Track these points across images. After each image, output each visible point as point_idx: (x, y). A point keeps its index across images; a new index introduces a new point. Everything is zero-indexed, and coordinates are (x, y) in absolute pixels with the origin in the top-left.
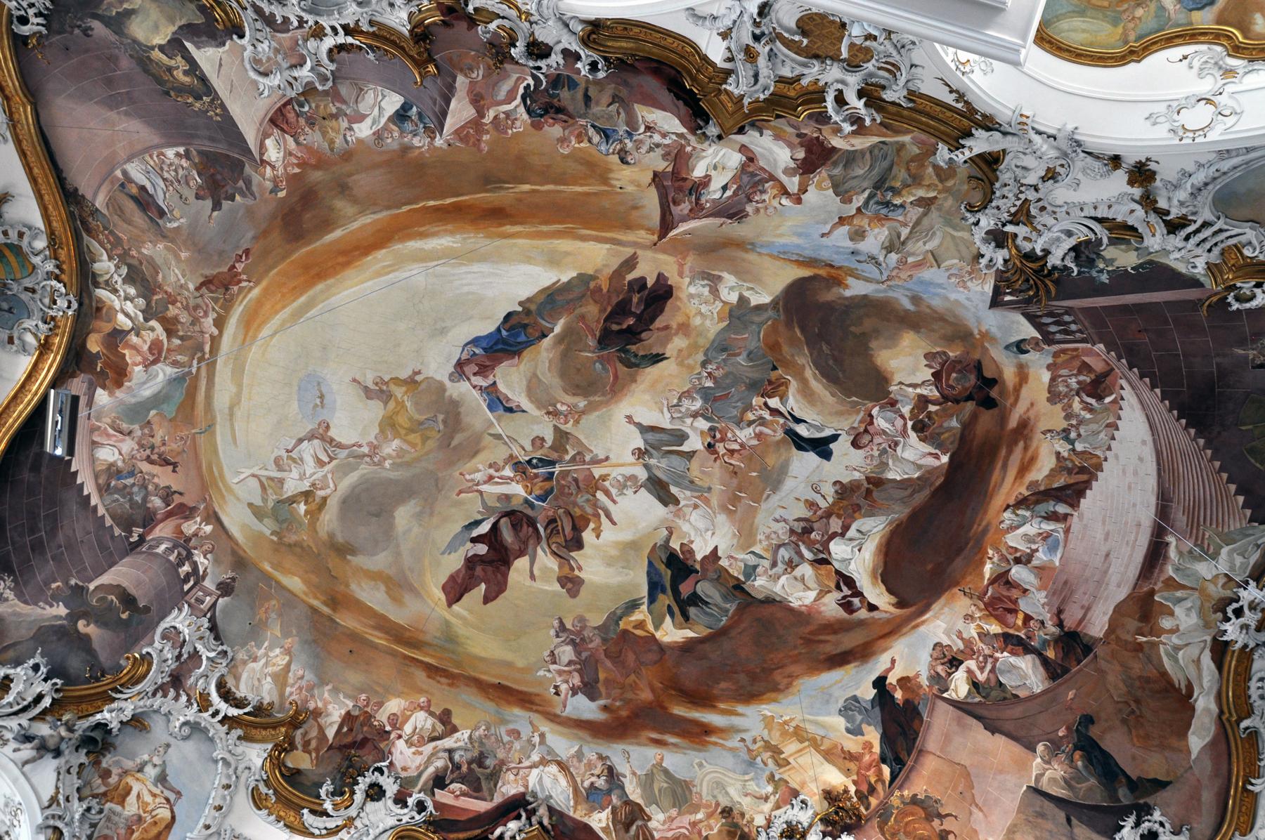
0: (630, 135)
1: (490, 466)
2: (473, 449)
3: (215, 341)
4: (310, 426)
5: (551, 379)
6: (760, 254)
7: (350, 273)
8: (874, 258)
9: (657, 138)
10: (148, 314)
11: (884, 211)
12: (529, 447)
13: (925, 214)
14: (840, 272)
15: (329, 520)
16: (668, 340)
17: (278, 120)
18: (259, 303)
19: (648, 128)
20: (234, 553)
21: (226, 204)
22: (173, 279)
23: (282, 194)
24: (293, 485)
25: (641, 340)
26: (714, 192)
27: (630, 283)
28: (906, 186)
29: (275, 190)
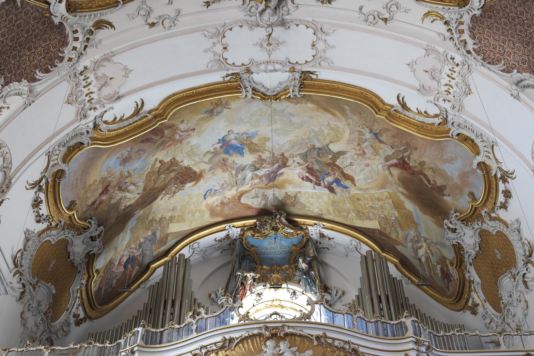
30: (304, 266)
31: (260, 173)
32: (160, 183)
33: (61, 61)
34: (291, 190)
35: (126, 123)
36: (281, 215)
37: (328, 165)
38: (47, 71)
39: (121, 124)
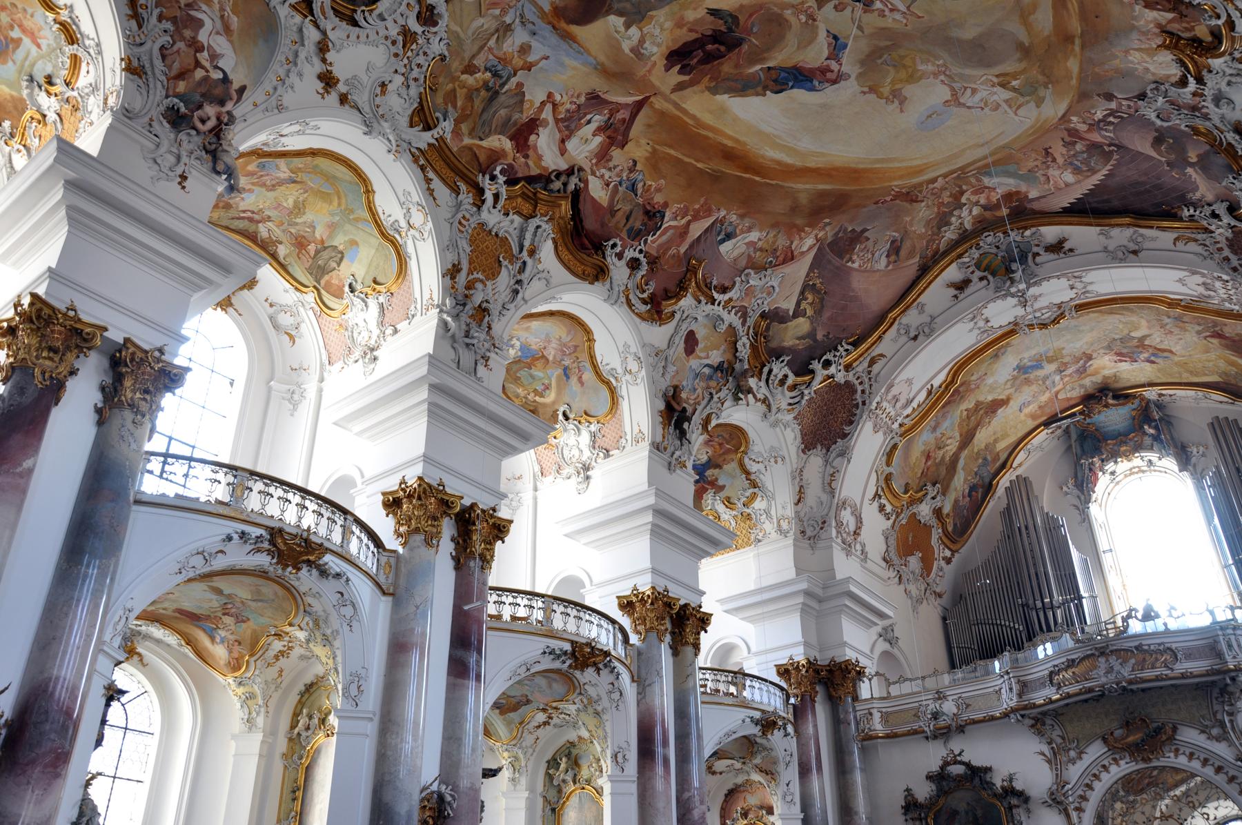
0: (620, 183)
1: (884, 16)
2: (883, 32)
3: (945, 176)
4: (955, 109)
5: (791, 39)
6: (595, 59)
7: (838, 163)
8: (522, 22)
9: (607, 175)
10: (961, 206)
11: (499, 67)
12: (849, 9)
13: (474, 57)
14: (551, 19)
15: (1009, 67)
16: (697, 21)
17: (789, 257)
18: (901, 177)
19: (608, 185)
20: (1078, 102)
21: (859, 229)
22: (927, 212)
23: (827, 220)
24: (1004, 94)
25: (714, 30)
26: (598, 120)
27: (689, 74)
28: (477, 90)
29: (829, 224)
30: (1152, 431)
31: (1068, 372)
32: (972, 425)
33: (857, 408)
34: (1107, 372)
35: (924, 406)
36: (1106, 396)
37: (1137, 347)
38: (851, 423)
39: (921, 409)
